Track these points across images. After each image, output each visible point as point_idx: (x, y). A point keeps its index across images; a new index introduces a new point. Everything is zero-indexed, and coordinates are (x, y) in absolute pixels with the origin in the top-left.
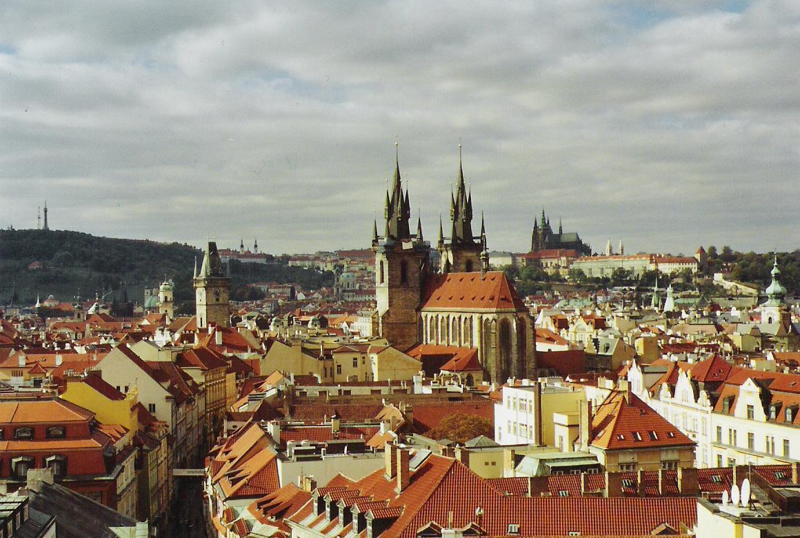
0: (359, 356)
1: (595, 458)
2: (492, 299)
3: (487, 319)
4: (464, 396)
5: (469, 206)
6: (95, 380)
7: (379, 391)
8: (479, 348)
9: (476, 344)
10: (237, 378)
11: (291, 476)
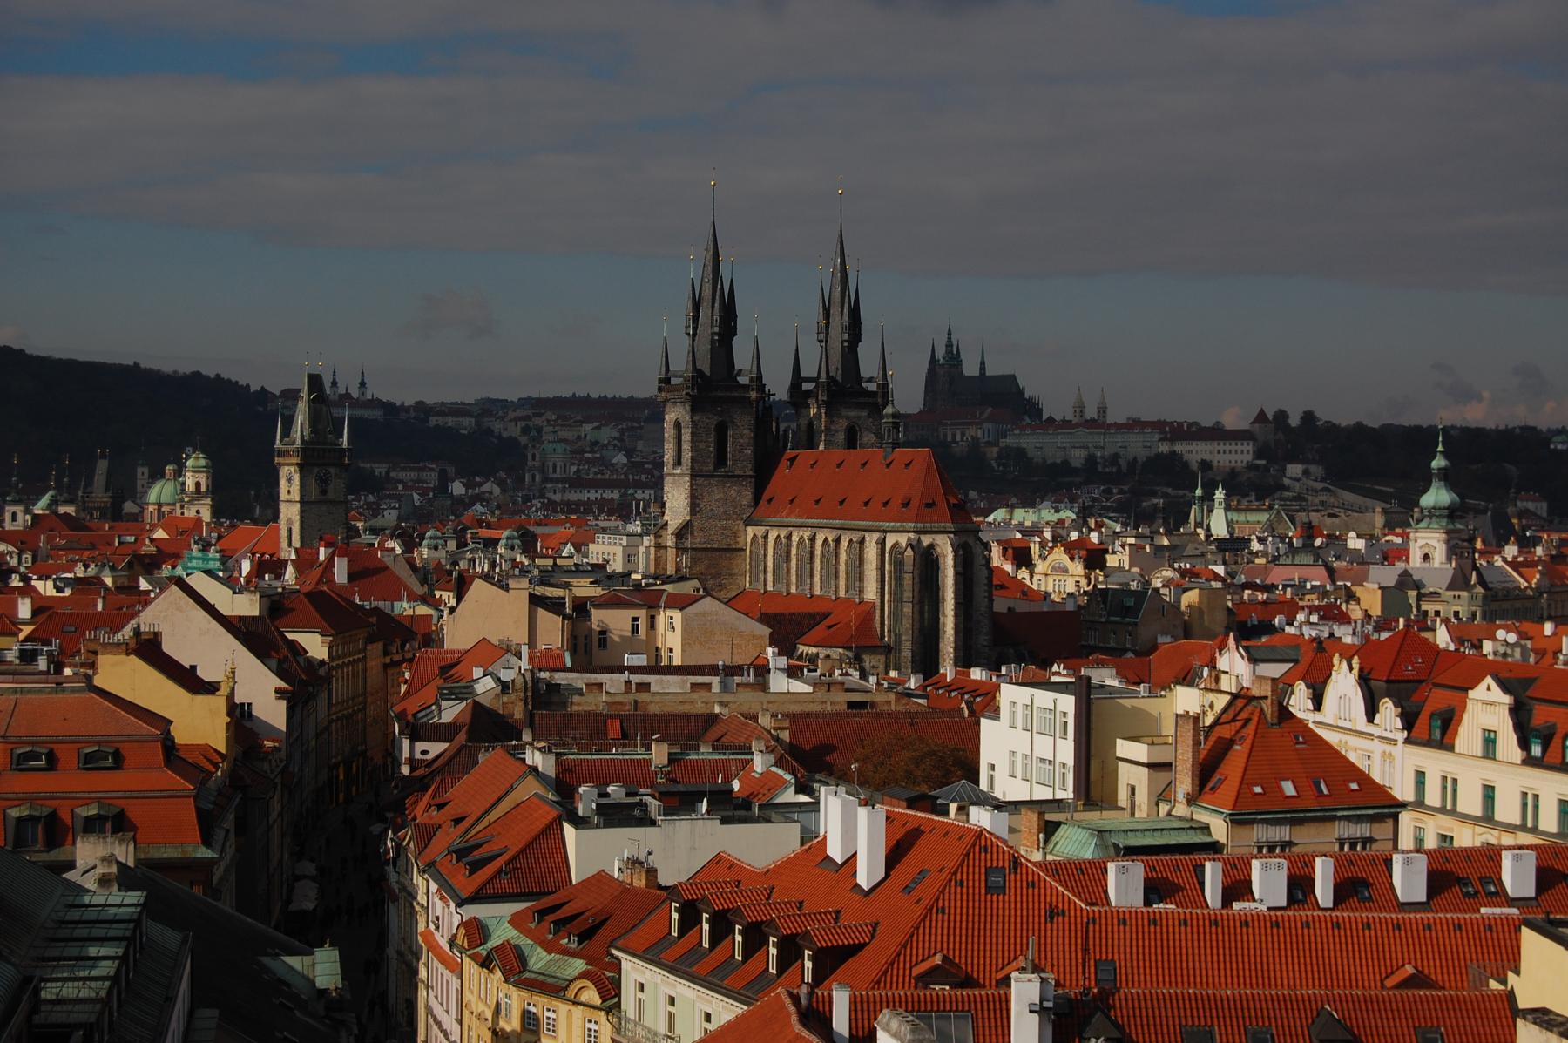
0: (642, 614)
1: (1206, 828)
2: (906, 504)
3: (896, 545)
4: (878, 698)
5: (855, 313)
6: (149, 649)
7: (708, 686)
8: (878, 603)
9: (871, 593)
10: (386, 653)
11: (589, 853)
